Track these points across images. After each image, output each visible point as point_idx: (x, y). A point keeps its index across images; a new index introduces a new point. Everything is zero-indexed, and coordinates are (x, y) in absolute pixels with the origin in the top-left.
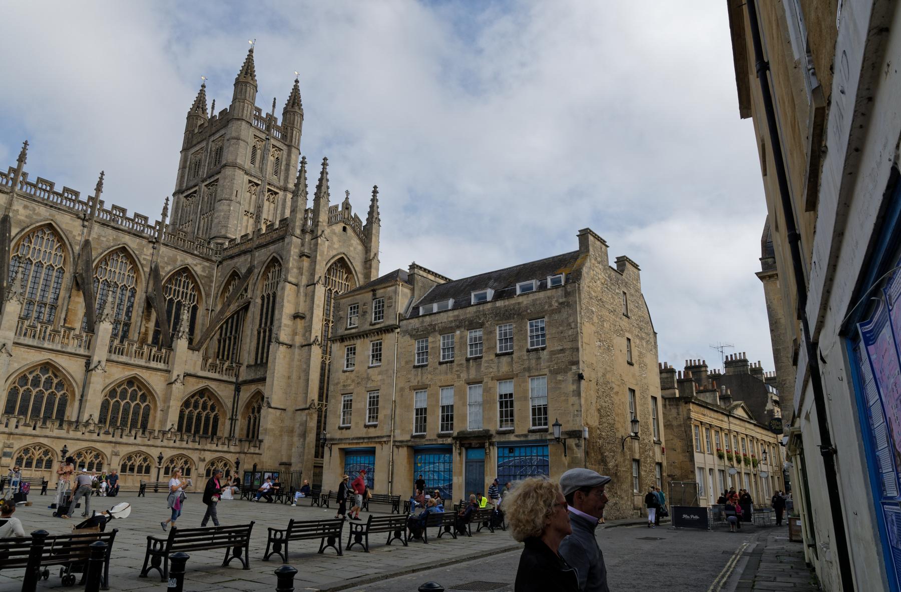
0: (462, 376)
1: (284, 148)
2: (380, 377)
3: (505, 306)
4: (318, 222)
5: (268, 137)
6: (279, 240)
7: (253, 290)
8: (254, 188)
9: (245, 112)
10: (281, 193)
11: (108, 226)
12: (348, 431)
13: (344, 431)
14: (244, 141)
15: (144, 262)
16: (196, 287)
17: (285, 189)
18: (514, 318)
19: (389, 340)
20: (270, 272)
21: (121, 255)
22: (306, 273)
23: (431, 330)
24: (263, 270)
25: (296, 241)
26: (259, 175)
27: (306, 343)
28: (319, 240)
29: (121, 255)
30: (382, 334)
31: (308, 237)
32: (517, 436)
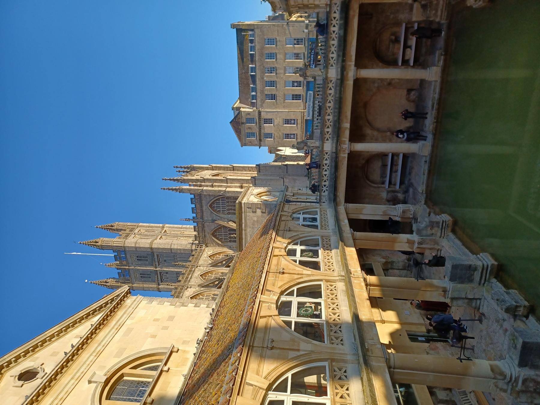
0: (282, 77)
1: (139, 228)
2: (278, 118)
3: (258, 56)
4: (196, 179)
5: (134, 233)
6: (201, 203)
7: (224, 218)
8: (163, 238)
9: (120, 241)
10: (165, 229)
11: (190, 280)
12: (298, 135)
13: (298, 137)
14: (137, 241)
15: (208, 269)
16: (219, 254)
17: (163, 227)
18: (263, 52)
19: (264, 116)
20: (216, 210)
21: (204, 277)
22: (221, 184)
23: (262, 92)
24: (216, 214)
25: (205, 188)
26: (156, 236)
27: (254, 182)
28: (205, 178)
29: (204, 277)
30: (261, 118)
31: (203, 184)
32: (306, 51)
